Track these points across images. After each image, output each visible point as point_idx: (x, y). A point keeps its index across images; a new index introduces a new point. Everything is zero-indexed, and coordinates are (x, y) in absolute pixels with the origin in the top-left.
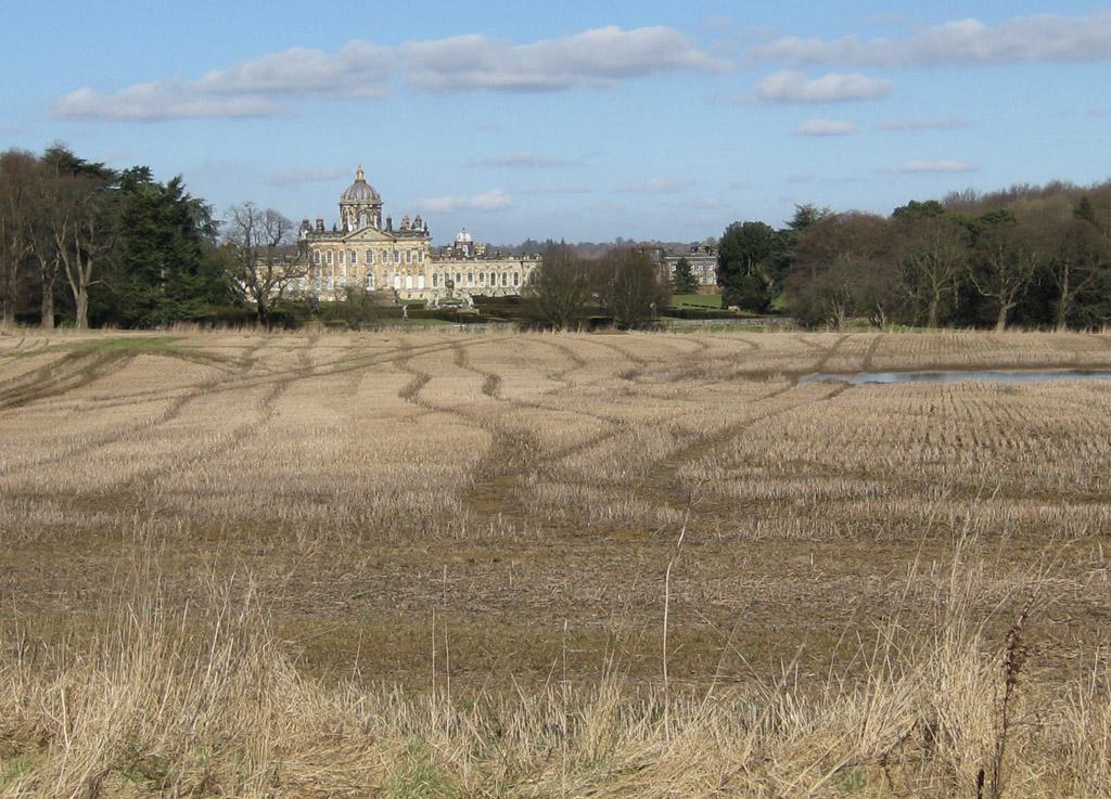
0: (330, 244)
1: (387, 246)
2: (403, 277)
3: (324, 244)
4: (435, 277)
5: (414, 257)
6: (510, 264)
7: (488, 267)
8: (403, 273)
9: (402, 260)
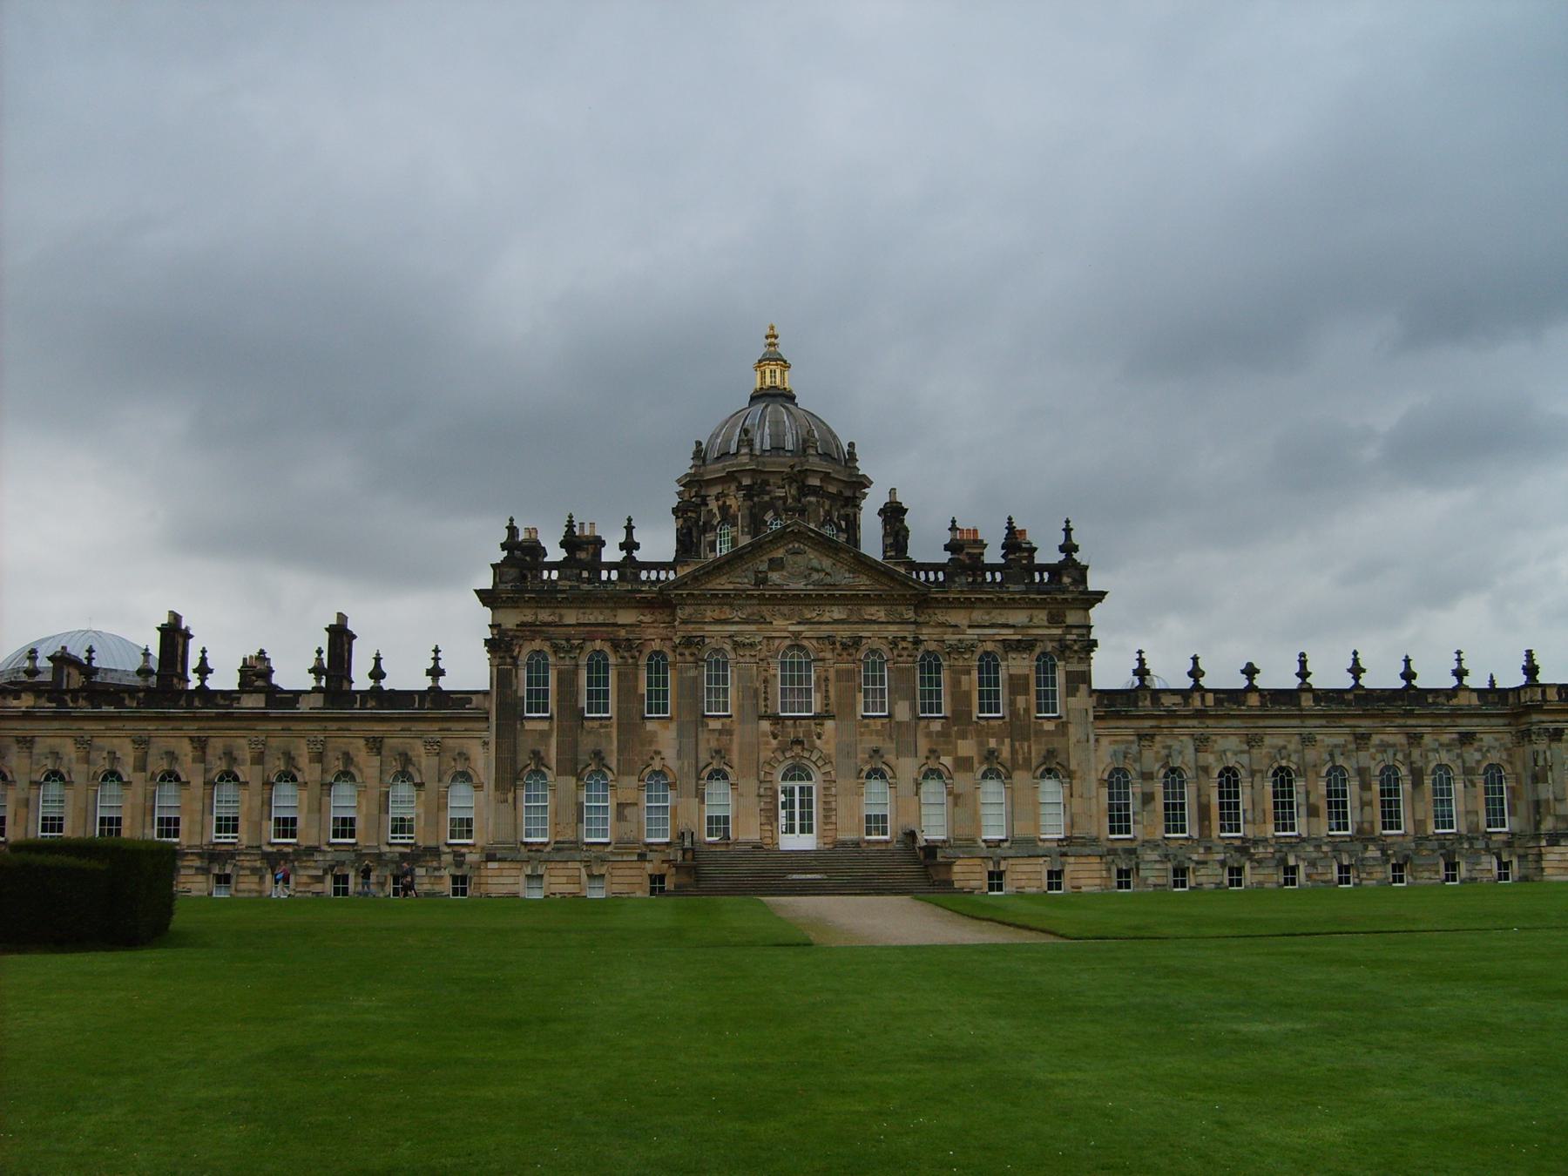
1: (881, 628)
2: (962, 782)
3: (571, 617)
4: (1117, 780)
5: (1018, 685)
6: (1466, 725)
8: (964, 764)
9: (960, 698)
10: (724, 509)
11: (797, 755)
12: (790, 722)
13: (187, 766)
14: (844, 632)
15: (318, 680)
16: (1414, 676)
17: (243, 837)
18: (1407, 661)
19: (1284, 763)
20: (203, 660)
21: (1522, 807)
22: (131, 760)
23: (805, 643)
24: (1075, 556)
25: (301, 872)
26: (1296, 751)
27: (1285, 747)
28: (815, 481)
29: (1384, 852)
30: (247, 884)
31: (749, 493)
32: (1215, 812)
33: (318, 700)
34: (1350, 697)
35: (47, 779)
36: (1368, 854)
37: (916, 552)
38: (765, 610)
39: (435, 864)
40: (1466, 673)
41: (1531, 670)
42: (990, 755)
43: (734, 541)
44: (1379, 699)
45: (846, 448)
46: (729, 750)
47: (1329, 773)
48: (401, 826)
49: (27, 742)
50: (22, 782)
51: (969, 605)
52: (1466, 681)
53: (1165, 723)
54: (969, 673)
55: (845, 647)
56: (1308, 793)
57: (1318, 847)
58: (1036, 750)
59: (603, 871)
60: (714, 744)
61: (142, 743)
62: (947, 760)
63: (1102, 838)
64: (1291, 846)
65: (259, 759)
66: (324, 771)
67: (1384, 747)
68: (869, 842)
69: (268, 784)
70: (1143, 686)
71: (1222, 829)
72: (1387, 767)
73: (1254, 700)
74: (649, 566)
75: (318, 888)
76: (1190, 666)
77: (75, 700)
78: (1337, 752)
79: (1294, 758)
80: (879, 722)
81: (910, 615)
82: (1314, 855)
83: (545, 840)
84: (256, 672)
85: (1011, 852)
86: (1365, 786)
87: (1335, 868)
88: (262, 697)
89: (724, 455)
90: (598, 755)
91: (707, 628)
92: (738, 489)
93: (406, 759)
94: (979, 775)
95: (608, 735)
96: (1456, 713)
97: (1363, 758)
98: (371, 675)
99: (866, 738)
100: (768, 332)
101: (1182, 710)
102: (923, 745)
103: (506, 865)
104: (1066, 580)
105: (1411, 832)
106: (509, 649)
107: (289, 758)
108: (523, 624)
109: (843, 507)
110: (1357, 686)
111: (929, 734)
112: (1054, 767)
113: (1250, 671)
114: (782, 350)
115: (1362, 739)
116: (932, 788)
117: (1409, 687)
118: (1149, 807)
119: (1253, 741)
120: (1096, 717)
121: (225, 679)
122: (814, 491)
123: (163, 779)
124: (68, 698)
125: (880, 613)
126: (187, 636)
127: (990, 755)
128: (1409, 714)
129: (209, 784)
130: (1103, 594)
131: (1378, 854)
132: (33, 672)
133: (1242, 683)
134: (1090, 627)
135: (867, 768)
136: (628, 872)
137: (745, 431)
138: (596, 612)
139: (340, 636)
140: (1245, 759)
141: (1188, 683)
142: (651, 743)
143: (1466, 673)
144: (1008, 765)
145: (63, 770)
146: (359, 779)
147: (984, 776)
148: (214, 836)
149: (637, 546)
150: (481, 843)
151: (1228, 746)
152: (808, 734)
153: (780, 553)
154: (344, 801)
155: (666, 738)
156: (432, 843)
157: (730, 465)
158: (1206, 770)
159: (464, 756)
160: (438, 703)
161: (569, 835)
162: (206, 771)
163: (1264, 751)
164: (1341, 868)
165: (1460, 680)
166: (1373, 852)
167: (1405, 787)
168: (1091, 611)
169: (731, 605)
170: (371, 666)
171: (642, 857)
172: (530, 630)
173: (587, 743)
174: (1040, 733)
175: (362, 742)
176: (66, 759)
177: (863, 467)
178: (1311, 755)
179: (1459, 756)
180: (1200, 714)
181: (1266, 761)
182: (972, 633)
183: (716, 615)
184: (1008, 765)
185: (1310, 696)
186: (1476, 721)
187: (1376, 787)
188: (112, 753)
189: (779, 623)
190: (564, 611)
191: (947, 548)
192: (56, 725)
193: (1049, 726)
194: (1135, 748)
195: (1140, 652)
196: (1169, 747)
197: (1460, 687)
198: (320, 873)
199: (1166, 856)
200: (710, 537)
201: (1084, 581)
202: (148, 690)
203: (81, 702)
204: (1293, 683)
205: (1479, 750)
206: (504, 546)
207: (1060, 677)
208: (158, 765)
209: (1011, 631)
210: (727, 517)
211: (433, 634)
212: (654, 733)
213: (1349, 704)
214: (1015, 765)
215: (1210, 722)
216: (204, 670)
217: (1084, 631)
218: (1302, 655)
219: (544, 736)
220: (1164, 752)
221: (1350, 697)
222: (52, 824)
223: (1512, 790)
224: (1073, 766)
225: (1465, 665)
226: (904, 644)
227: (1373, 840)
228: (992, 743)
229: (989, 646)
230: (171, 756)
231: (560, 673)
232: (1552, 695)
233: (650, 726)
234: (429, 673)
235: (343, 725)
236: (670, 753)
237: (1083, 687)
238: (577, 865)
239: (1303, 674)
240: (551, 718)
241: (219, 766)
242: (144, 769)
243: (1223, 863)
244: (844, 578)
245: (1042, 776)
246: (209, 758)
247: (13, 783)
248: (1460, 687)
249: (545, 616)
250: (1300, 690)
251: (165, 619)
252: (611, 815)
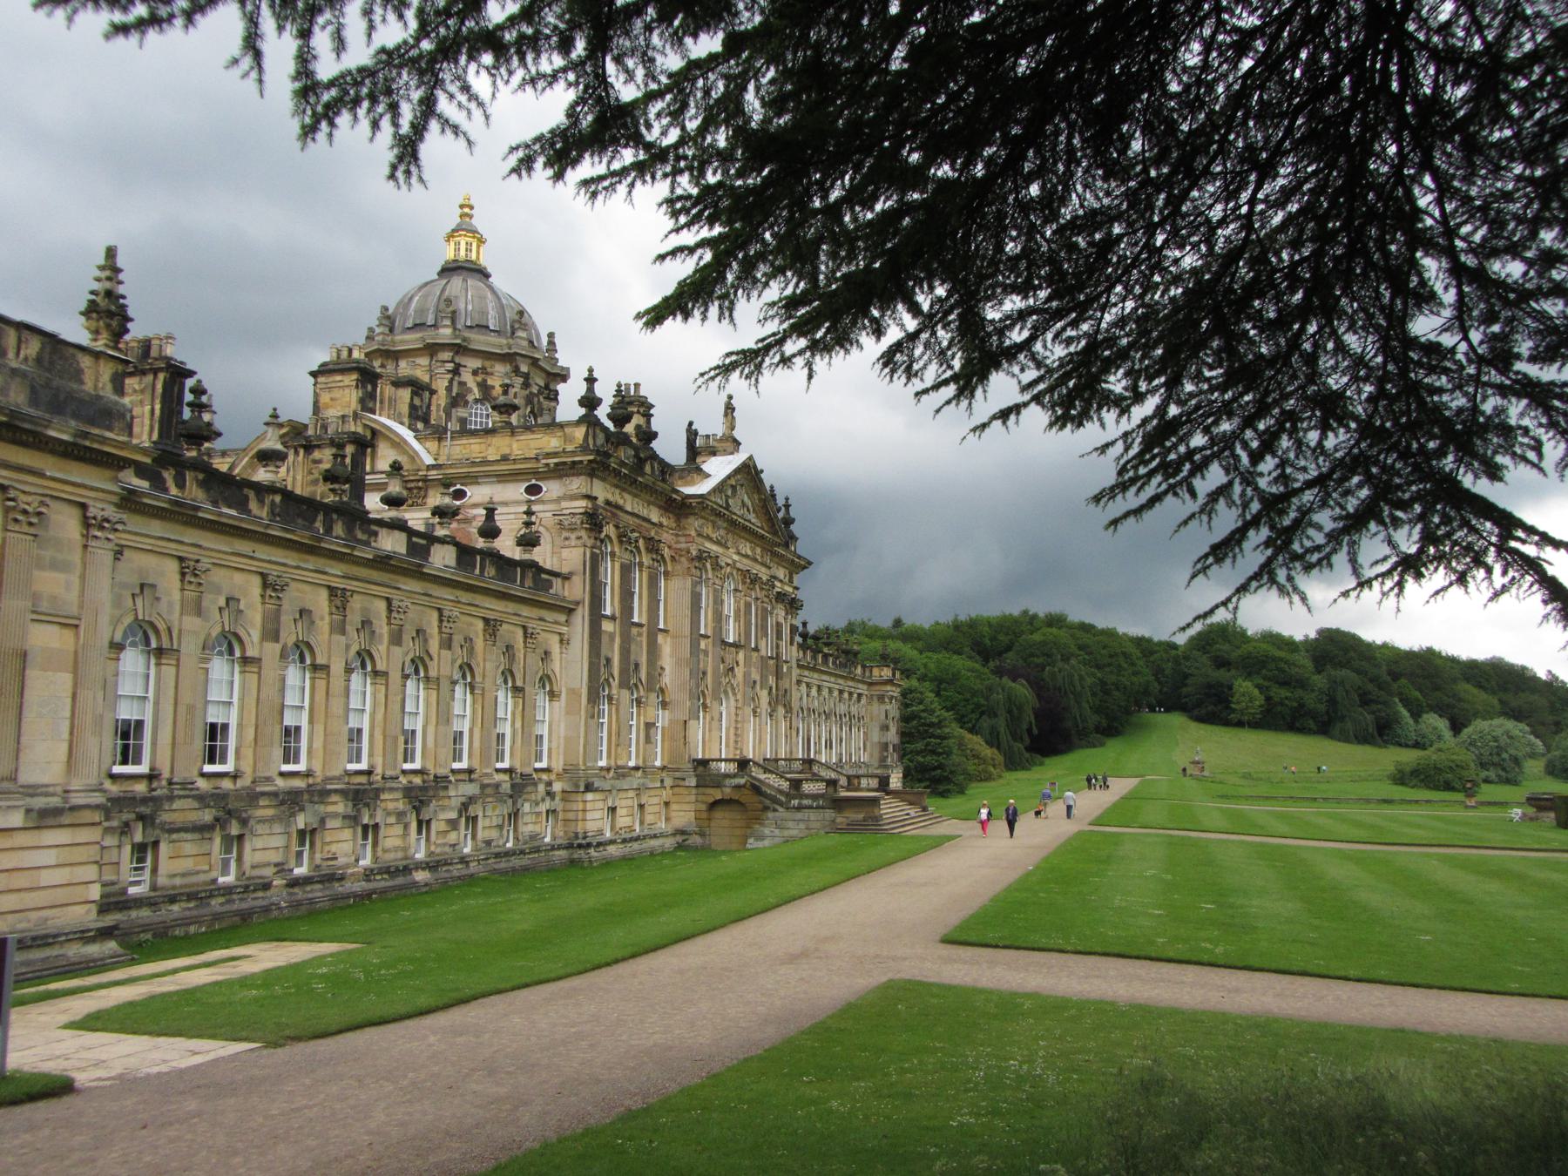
22: (258, 619)
100: (462, 202)
108: (608, 503)
130: (810, 563)
169: (714, 523)
175: (480, 625)
176: (164, 600)
190: (627, 496)
231: (623, 566)
242: (276, 637)
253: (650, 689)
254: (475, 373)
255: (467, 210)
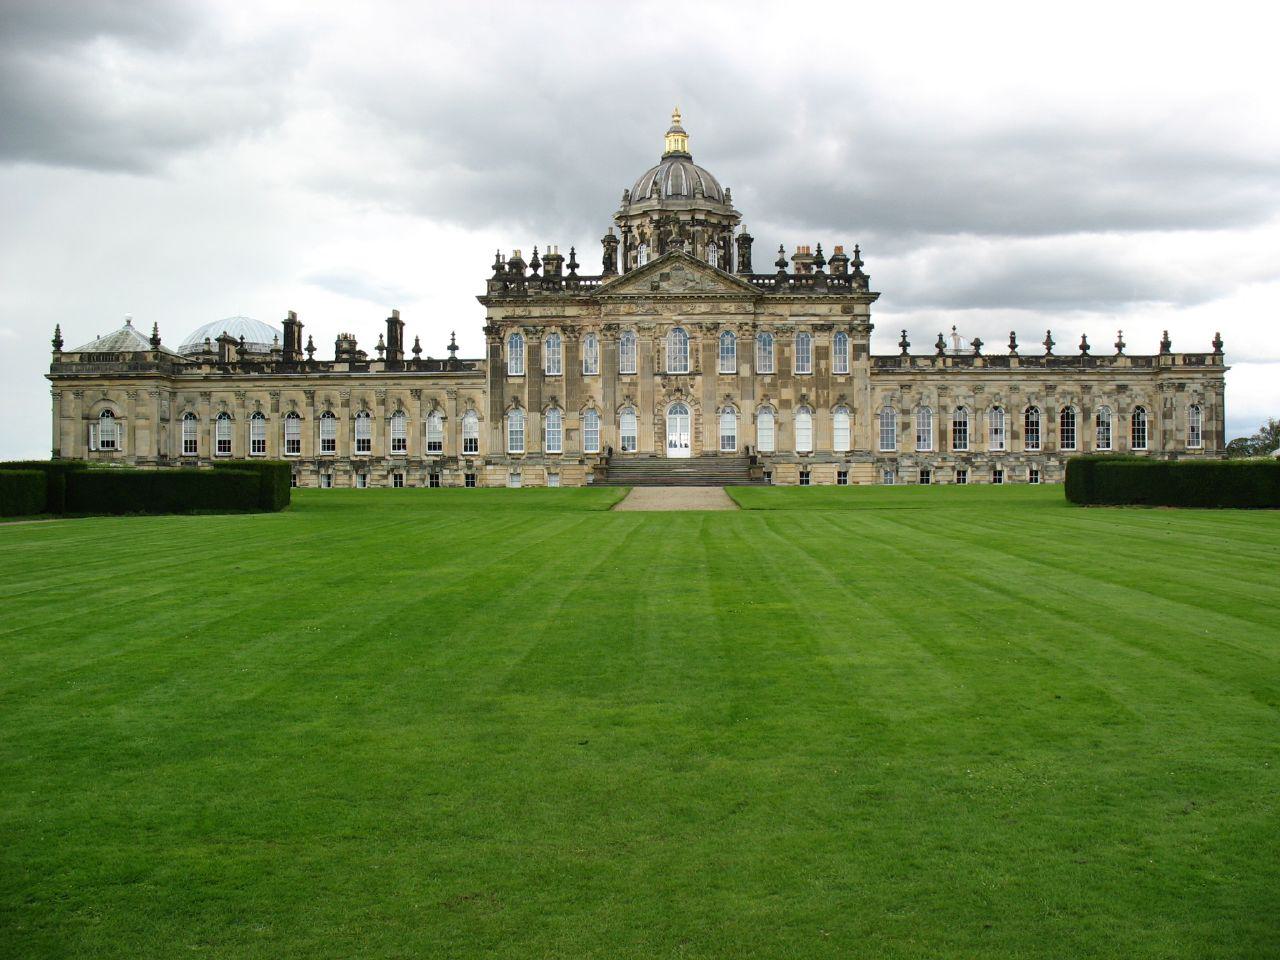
0: (551, 311)
1: (732, 315)
2: (784, 415)
3: (536, 311)
4: (884, 417)
6: (1122, 380)
7: (1050, 388)
8: (785, 404)
9: (784, 362)
10: (642, 235)
11: (678, 398)
12: (674, 378)
13: (303, 409)
14: (708, 320)
15: (381, 354)
16: (1088, 347)
17: (339, 452)
18: (1084, 337)
19: (997, 404)
20: (310, 343)
21: (1158, 435)
23: (683, 327)
24: (861, 269)
25: (374, 473)
26: (1006, 396)
27: (998, 394)
28: (701, 217)
29: (1061, 462)
30: (341, 481)
31: (658, 225)
32: (950, 435)
33: (381, 366)
34: (1043, 361)
35: (220, 418)
36: (1051, 463)
37: (757, 269)
38: (659, 307)
39: (455, 467)
40: (1124, 345)
41: (1166, 345)
42: (803, 399)
43: (648, 256)
44: (1064, 362)
45: (724, 192)
46: (634, 396)
47: (1027, 411)
48: (434, 446)
49: (207, 395)
50: (205, 419)
51: (789, 301)
52: (1125, 351)
53: (919, 377)
54: (789, 345)
55: (709, 329)
56: (1012, 424)
57: (1017, 458)
58: (833, 395)
59: (558, 471)
60: (625, 392)
61: (275, 395)
62: (774, 402)
63: (875, 451)
64: (999, 457)
65: (346, 404)
66: (386, 411)
67: (1064, 394)
68: (723, 453)
69: (352, 418)
70: (905, 353)
71: (955, 447)
72: (1067, 408)
73: (978, 362)
74: (585, 279)
75: (384, 482)
76: (937, 340)
77: (234, 368)
78: (1033, 397)
79: (1004, 401)
80: (730, 377)
81: (750, 308)
82: (1013, 464)
83: (522, 452)
84: (347, 348)
85: (814, 460)
86: (1051, 419)
87: (1028, 472)
88: (347, 365)
89: (642, 199)
90: (554, 399)
91: (621, 318)
92: (651, 222)
93: (436, 403)
94: (795, 411)
95: (560, 386)
96: (1112, 373)
97: (1051, 401)
98: (413, 351)
99: (722, 387)
101: (931, 370)
102: (759, 392)
103: (497, 467)
104: (854, 285)
105: (1081, 450)
106: (498, 332)
107: (365, 403)
108: (506, 317)
109: (722, 232)
110: (1049, 354)
111: (763, 385)
112: (843, 402)
113: (977, 344)
114: (684, 126)
115: (1050, 388)
116: (766, 421)
117: (1085, 354)
118: (906, 432)
119: (977, 390)
120: (872, 374)
121: (325, 353)
122: (700, 223)
123: (289, 417)
124: (230, 367)
125: (732, 307)
126: (300, 326)
127: (803, 399)
128: (1083, 373)
129: (317, 418)
131: (1057, 463)
132: (209, 352)
133: (970, 350)
134: (869, 316)
135: (722, 406)
136: (573, 472)
137: (655, 183)
138: (552, 309)
139: (395, 325)
140: (971, 401)
141: (934, 352)
142: (587, 391)
143: (1124, 345)
144: (814, 404)
145: (229, 412)
146: (407, 415)
147: (799, 412)
148: (322, 452)
149: (577, 266)
150: (483, 454)
151: (960, 388)
152: (685, 385)
153: (666, 270)
154: (398, 429)
155: (597, 389)
156: (454, 455)
157: (645, 206)
158: (944, 408)
159: (472, 400)
160: (455, 367)
161: (536, 449)
162: (315, 411)
163: (984, 396)
164: (1031, 473)
165: (1120, 350)
166: (1054, 462)
167: (1078, 420)
168: (872, 305)
169: (636, 304)
170: (413, 345)
171: (581, 462)
172: (510, 320)
173: (547, 391)
174: (835, 384)
176: (230, 407)
177: (737, 204)
178: (1015, 398)
179: (1116, 400)
180: (942, 372)
181: (986, 403)
182: (792, 321)
183: (626, 310)
184: (814, 404)
185: (1017, 360)
186: (1129, 377)
187: (1058, 420)
188: (258, 401)
189: (667, 314)
191: (777, 264)
192: (224, 384)
193: (841, 380)
194: (898, 394)
195: (904, 331)
196: (921, 393)
197: (1120, 355)
198: (385, 473)
199: (916, 463)
200: (634, 253)
201: (866, 285)
202: (277, 362)
203: (238, 370)
204: (1007, 351)
205: (1131, 396)
206: (494, 268)
207: (849, 348)
208: (286, 408)
209: (817, 318)
210: (643, 240)
211: (451, 322)
212: (588, 385)
213: (1042, 366)
214: (818, 405)
215: (948, 377)
216: (311, 349)
217: (865, 318)
218: (1013, 333)
219: (521, 386)
220: (918, 396)
221: (1043, 361)
222: (224, 445)
223: (1151, 422)
224: (856, 405)
225: (1123, 340)
226: (746, 327)
227: (1054, 454)
228: (804, 391)
229: (803, 328)
230: (294, 402)
232: (1179, 361)
233: (587, 380)
234: (449, 348)
235: (396, 381)
236: (599, 397)
237: (864, 355)
238: (542, 467)
239: (1013, 346)
240: (524, 376)
241: (322, 408)
242: (277, 411)
243: (953, 468)
244: (710, 286)
245: (837, 412)
246: (316, 403)
247: (200, 420)
248: (1120, 355)
249: (519, 311)
250: (1010, 356)
251: (286, 317)
252: (562, 436)
253: (568, 410)
254: (638, 227)
255: (676, 118)
